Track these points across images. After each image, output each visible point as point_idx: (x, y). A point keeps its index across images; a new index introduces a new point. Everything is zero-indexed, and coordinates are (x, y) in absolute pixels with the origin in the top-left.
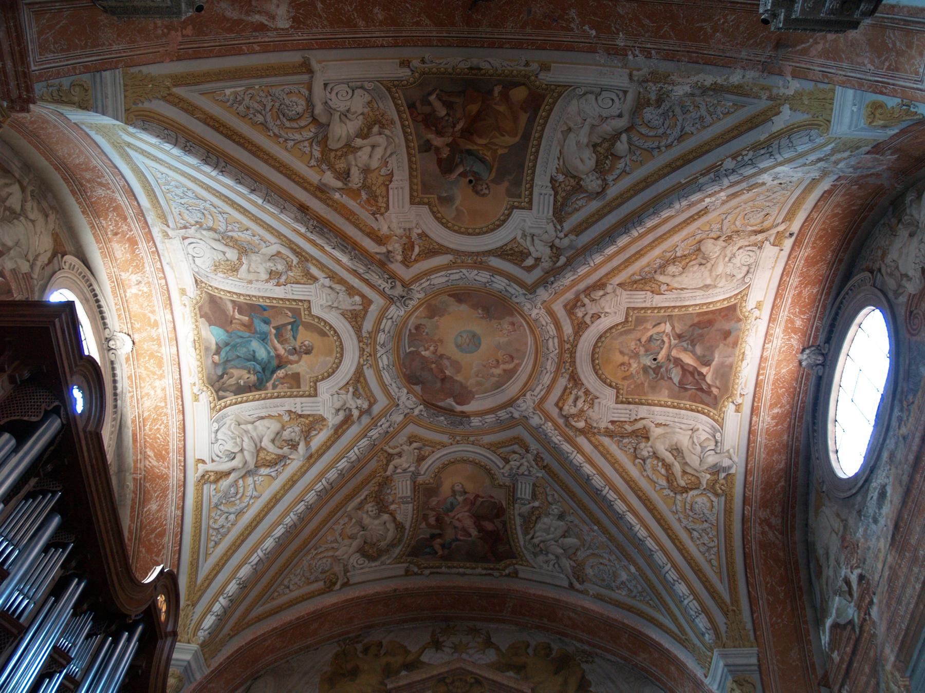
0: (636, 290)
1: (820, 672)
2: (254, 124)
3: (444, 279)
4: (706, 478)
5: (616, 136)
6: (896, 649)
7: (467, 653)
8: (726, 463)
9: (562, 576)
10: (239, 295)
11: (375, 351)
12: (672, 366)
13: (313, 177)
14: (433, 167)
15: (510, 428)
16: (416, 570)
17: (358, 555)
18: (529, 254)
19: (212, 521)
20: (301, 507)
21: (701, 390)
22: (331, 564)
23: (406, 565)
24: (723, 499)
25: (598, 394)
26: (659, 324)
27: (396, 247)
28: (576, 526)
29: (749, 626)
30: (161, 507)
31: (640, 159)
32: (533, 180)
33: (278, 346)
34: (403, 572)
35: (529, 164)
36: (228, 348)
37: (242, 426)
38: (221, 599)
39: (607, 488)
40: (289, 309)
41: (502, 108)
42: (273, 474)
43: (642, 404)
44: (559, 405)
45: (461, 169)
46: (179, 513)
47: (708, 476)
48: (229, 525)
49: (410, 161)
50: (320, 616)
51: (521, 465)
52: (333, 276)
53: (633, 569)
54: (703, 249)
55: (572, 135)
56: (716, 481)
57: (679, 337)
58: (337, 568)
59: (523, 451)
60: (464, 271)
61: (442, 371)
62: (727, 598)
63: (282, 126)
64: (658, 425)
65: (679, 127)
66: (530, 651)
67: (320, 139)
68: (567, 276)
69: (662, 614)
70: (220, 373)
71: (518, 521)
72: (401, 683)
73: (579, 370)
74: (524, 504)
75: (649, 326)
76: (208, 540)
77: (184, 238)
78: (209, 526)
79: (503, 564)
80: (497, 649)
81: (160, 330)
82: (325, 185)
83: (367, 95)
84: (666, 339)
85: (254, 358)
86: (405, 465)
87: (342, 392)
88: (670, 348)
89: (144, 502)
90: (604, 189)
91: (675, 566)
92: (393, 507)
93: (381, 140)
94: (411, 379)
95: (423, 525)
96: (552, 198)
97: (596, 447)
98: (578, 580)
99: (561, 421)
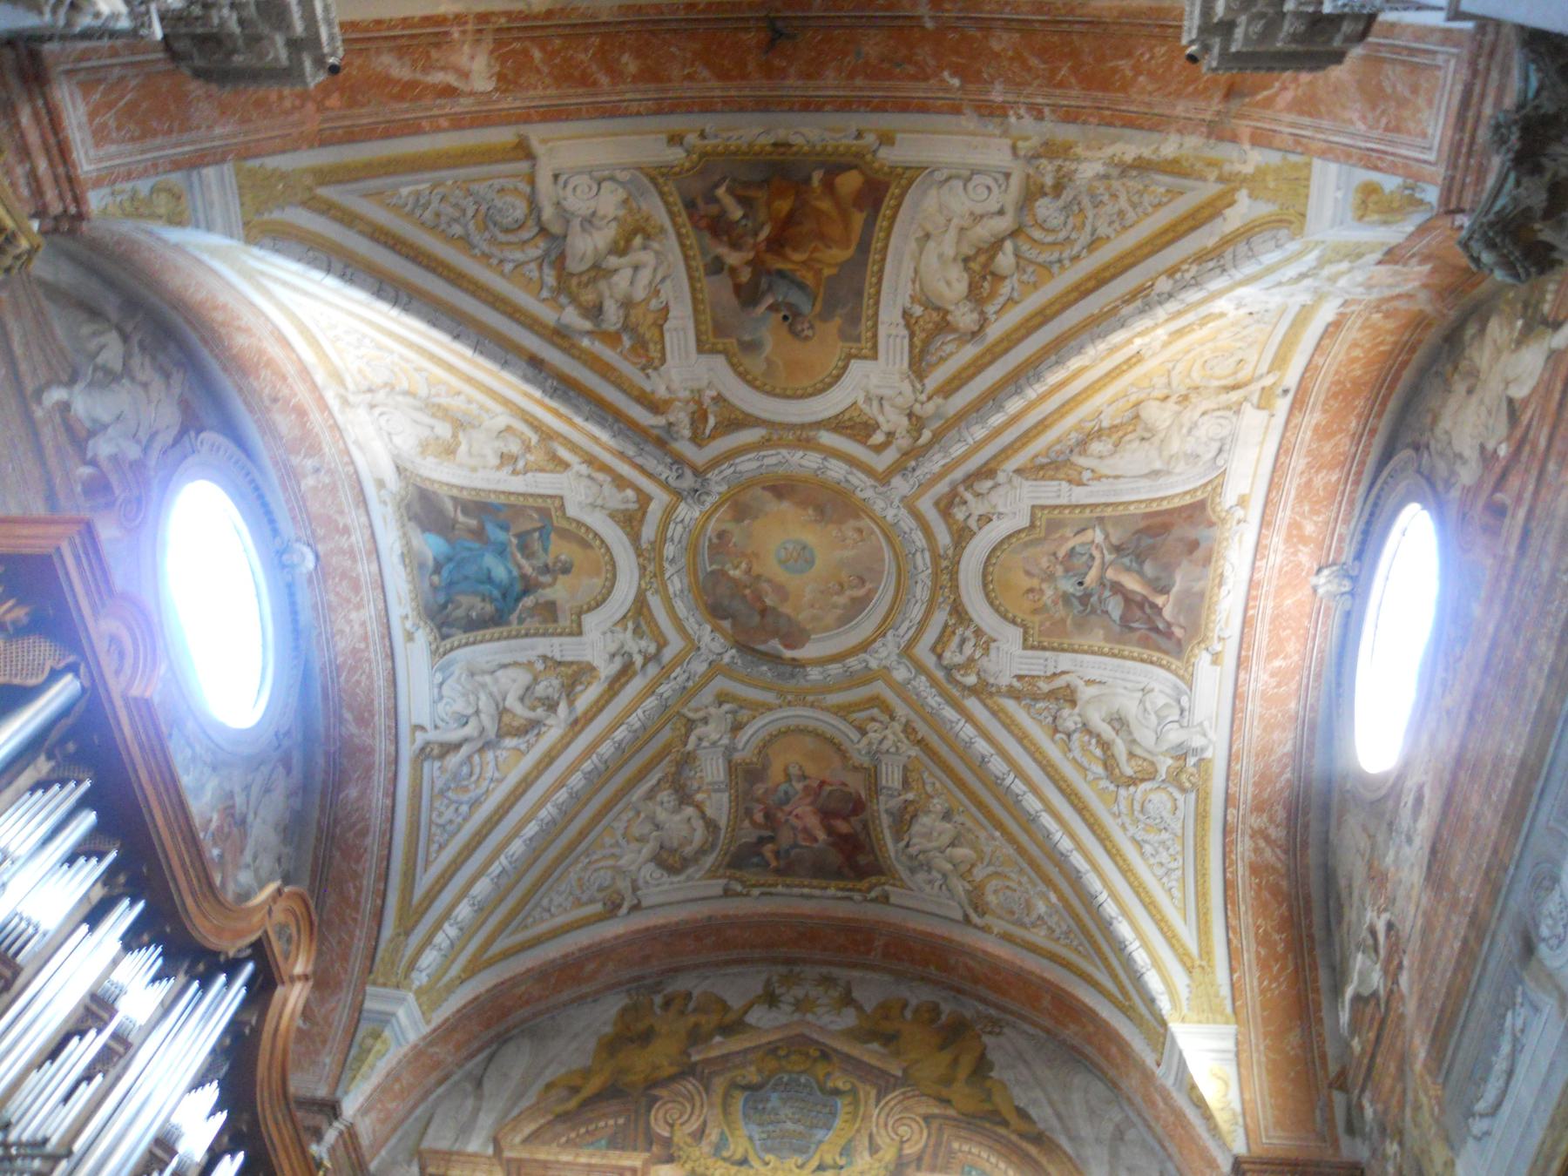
0: (1043, 478)
1: (1333, 1069)
2: (450, 239)
3: (755, 465)
4: (1165, 764)
5: (996, 245)
6: (1427, 1041)
7: (814, 1013)
8: (1197, 742)
9: (952, 903)
10: (462, 488)
11: (662, 570)
12: (1107, 593)
13: (548, 315)
14: (728, 298)
15: (864, 683)
16: (739, 888)
17: (652, 866)
18: (877, 426)
19: (434, 815)
20: (562, 795)
21: (1156, 630)
22: (613, 879)
23: (723, 882)
24: (1193, 796)
25: (994, 635)
26: (1083, 530)
27: (681, 417)
28: (969, 830)
29: (1225, 991)
30: (363, 794)
31: (1032, 279)
32: (876, 314)
33: (523, 562)
34: (719, 891)
35: (869, 290)
36: (451, 566)
37: (478, 678)
38: (446, 926)
39: (1012, 776)
40: (532, 508)
41: (825, 205)
42: (523, 747)
43: (1063, 650)
44: (937, 649)
45: (769, 300)
46: (388, 802)
47: (1170, 762)
48: (460, 820)
49: (693, 290)
50: (599, 953)
51: (885, 738)
52: (591, 460)
53: (1053, 898)
54: (1144, 415)
55: (931, 244)
56: (1181, 770)
57: (1118, 549)
58: (623, 885)
59: (885, 718)
60: (784, 452)
61: (759, 598)
62: (1193, 948)
63: (493, 241)
64: (1089, 682)
65: (1088, 229)
66: (908, 1014)
67: (553, 257)
68: (935, 458)
69: (1096, 966)
70: (441, 599)
71: (885, 820)
72: (713, 1053)
73: (965, 599)
74: (892, 796)
75: (1068, 532)
76: (430, 840)
77: (372, 406)
78: (431, 822)
79: (864, 884)
80: (860, 1008)
81: (353, 538)
82: (567, 327)
83: (620, 190)
84: (1096, 554)
85: (489, 579)
86: (715, 736)
87: (618, 628)
88: (1104, 567)
89: (339, 786)
90: (982, 328)
92: (699, 797)
93: (648, 257)
94: (716, 612)
95: (747, 823)
96: (906, 342)
97: (994, 714)
98: (976, 909)
99: (940, 675)
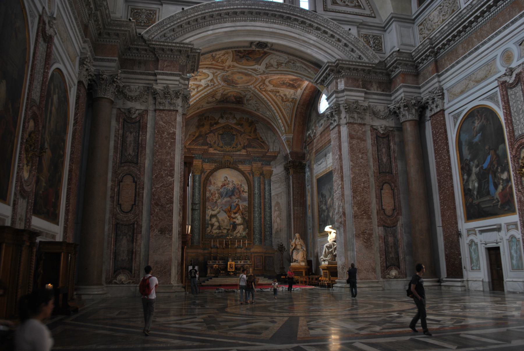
1: (305, 140)
4: (290, 100)
20: (195, 101)
29: (293, 130)
44: (259, 87)
62: (289, 123)
72: (215, 128)
80: (236, 119)
91: (280, 116)
